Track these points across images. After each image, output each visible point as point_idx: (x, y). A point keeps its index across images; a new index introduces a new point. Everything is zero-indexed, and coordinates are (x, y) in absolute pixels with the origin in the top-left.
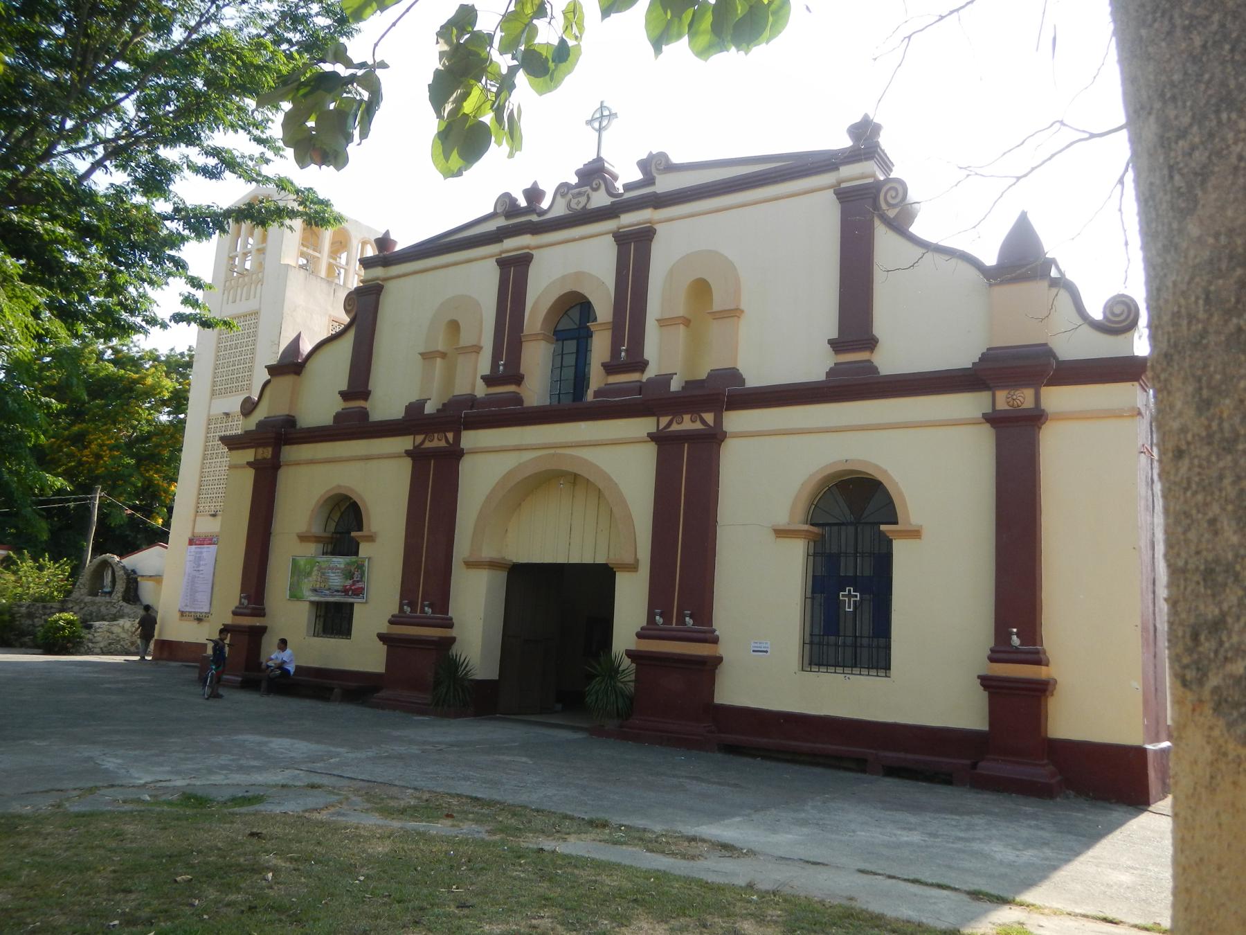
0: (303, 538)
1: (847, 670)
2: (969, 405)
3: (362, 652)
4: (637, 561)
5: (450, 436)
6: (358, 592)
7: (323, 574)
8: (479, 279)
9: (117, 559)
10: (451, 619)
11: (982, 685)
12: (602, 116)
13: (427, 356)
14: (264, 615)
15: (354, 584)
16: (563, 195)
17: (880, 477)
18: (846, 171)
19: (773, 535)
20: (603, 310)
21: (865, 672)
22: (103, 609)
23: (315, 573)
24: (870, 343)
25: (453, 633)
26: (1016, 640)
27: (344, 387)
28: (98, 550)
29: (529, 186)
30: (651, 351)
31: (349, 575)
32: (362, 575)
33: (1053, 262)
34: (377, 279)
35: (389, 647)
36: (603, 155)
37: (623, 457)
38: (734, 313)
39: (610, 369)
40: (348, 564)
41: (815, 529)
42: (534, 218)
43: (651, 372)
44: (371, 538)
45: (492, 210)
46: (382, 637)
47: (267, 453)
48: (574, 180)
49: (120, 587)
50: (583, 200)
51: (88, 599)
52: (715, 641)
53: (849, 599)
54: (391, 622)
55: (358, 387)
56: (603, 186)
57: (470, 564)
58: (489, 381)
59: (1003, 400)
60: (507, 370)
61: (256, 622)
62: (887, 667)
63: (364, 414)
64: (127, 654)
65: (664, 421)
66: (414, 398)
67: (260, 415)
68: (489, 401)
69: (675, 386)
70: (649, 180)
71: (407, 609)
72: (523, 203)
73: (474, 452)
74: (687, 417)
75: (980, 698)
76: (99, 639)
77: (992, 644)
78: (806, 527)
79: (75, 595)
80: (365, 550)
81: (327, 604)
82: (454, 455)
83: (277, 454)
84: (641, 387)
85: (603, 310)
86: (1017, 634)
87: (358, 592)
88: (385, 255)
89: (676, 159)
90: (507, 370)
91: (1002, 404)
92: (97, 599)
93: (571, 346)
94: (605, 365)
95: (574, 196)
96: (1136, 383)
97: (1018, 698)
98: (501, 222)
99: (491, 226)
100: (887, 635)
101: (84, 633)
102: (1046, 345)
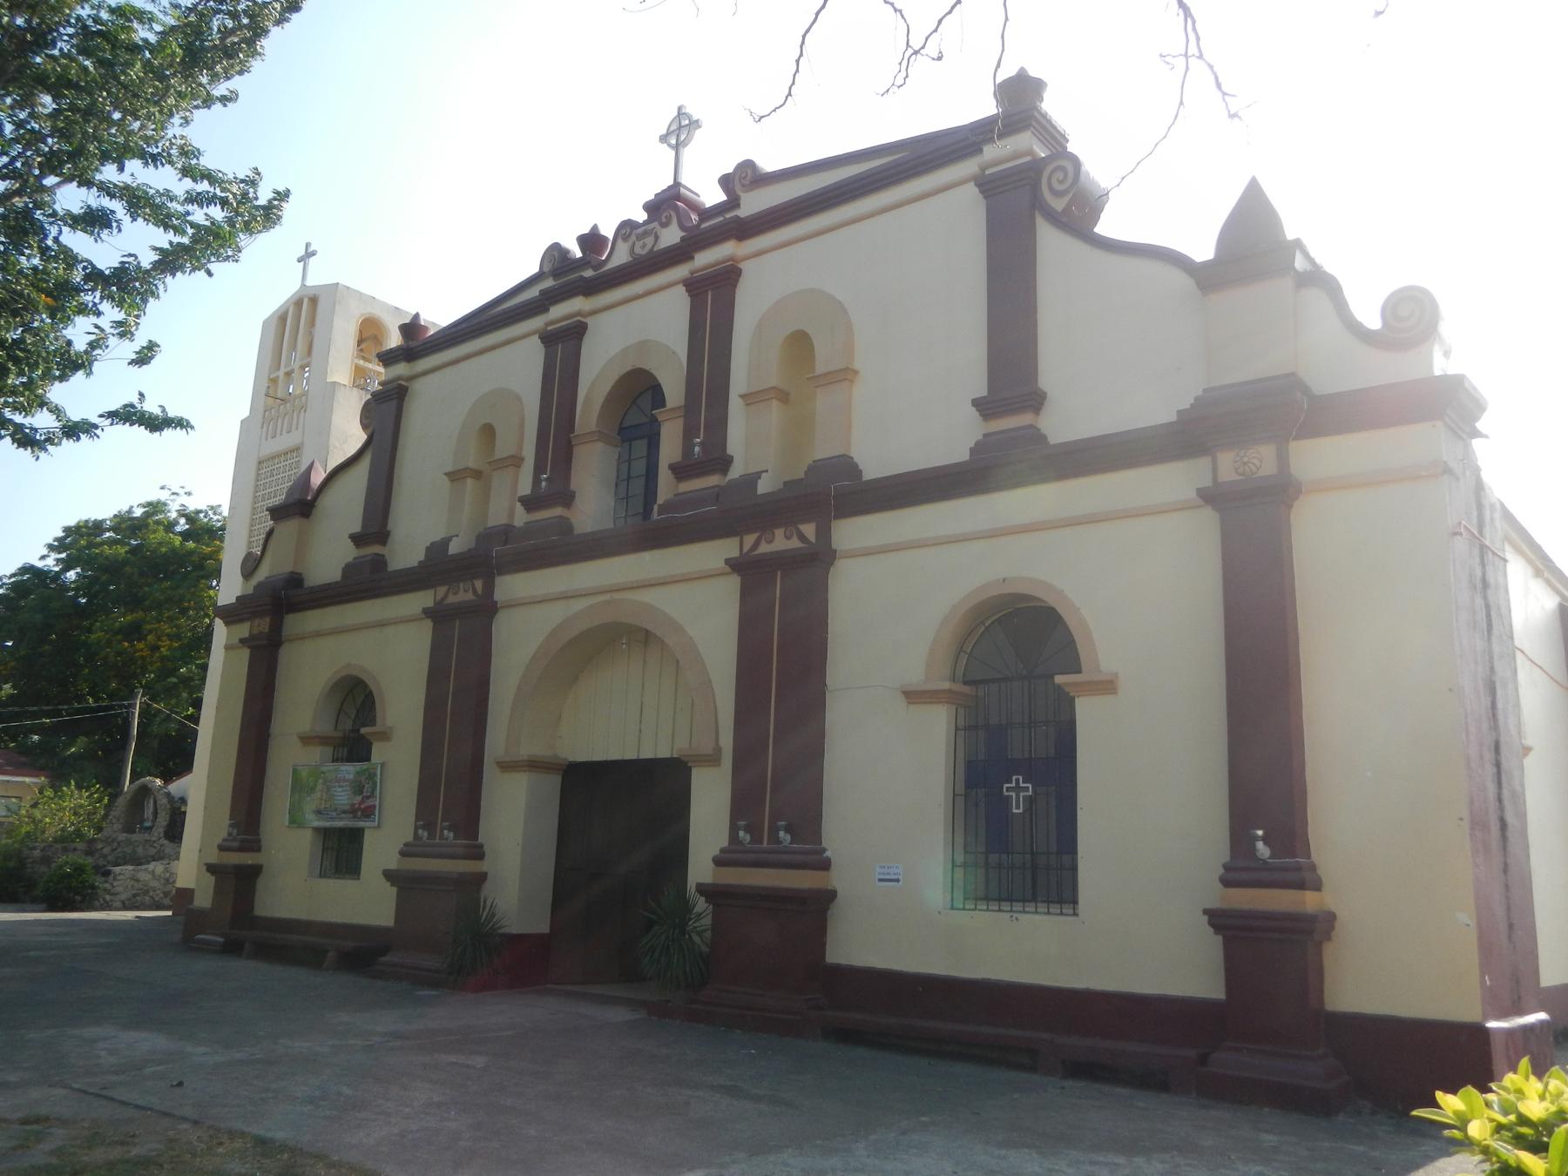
0: (306, 740)
1: (1018, 906)
2: (1173, 481)
3: (367, 901)
4: (718, 750)
5: (479, 584)
8: (519, 364)
9: (158, 782)
10: (481, 846)
11: (1211, 924)
12: (680, 127)
13: (455, 476)
14: (259, 850)
16: (625, 239)
17: (1051, 601)
20: (674, 392)
21: (1042, 908)
22: (140, 850)
23: (319, 787)
24: (1035, 401)
25: (484, 866)
26: (1262, 849)
27: (356, 528)
28: (135, 776)
29: (586, 230)
30: (736, 440)
31: (358, 789)
33: (1298, 244)
34: (399, 378)
35: (400, 889)
36: (684, 180)
37: (695, 599)
38: (846, 375)
39: (681, 471)
40: (358, 773)
41: (966, 689)
42: (588, 273)
43: (736, 472)
44: (385, 736)
45: (535, 269)
46: (389, 875)
47: (263, 625)
48: (641, 216)
49: (163, 819)
50: (649, 241)
51: (122, 837)
52: (825, 865)
53: (1018, 793)
54: (403, 854)
55: (375, 529)
56: (675, 220)
57: (507, 766)
58: (530, 503)
59: (1228, 466)
60: (554, 486)
61: (248, 859)
62: (1074, 902)
63: (379, 563)
64: (158, 908)
65: (750, 540)
66: (437, 535)
67: (263, 573)
68: (529, 529)
69: (764, 487)
70: (733, 202)
71: (424, 834)
72: (578, 253)
73: (511, 605)
74: (779, 533)
75: (1212, 946)
76: (120, 889)
77: (1225, 857)
78: (958, 687)
79: (107, 832)
80: (378, 753)
81: (341, 830)
82: (487, 609)
83: (277, 627)
84: (718, 494)
85: (674, 392)
86: (1265, 839)
87: (368, 813)
88: (418, 343)
90: (554, 486)
91: (1227, 474)
92: (135, 837)
93: (640, 447)
94: (673, 468)
95: (639, 237)
96: (1439, 424)
97: (1271, 945)
98: (549, 283)
99: (533, 293)
100: (1073, 850)
101: (98, 881)
102: (1293, 374)
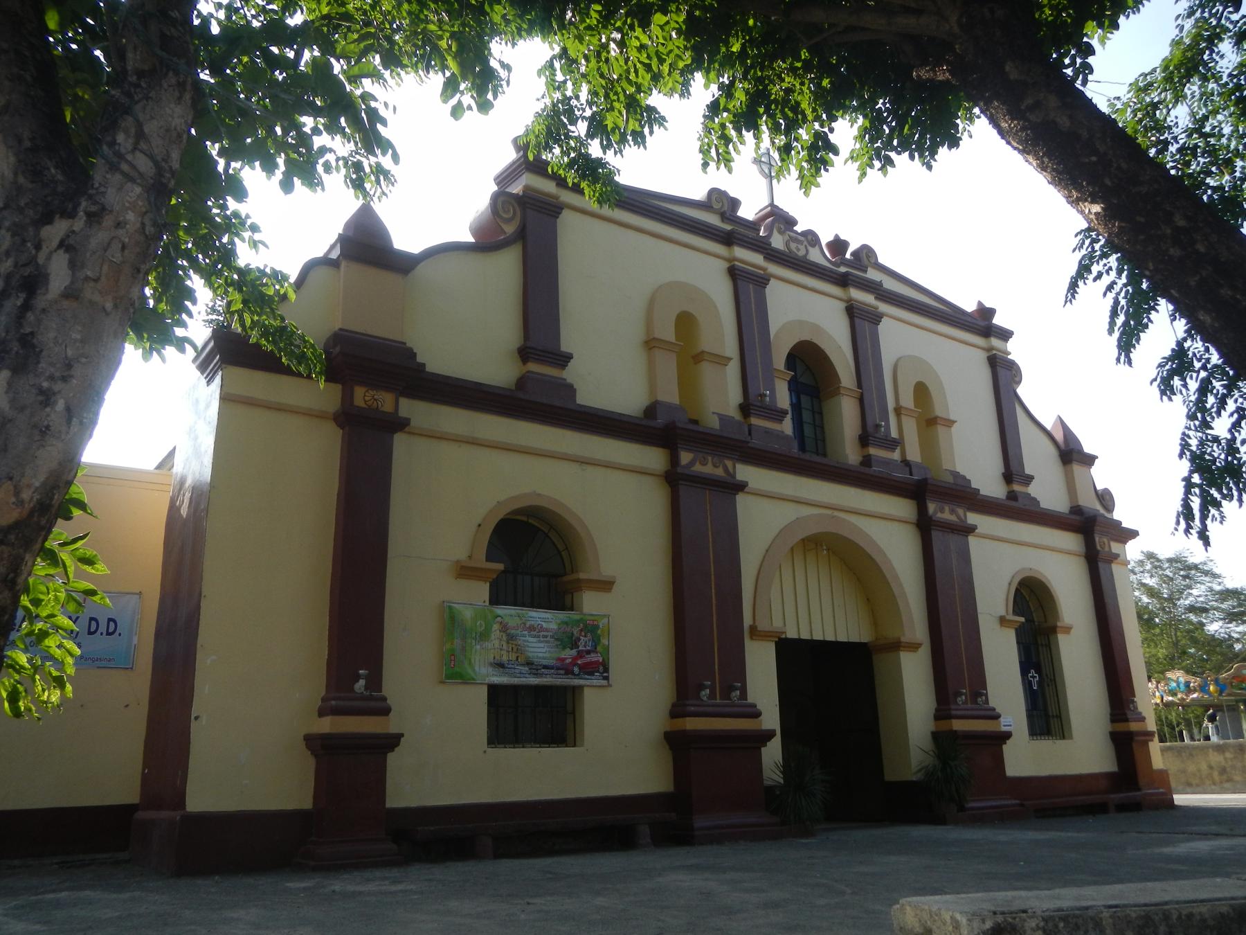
0: (465, 572)
6: (600, 669)
7: (511, 638)
15: (580, 655)
18: (995, 342)
19: (997, 626)
32: (596, 641)
38: (950, 423)
40: (566, 623)
44: (606, 585)
80: (591, 603)
89: (881, 260)
